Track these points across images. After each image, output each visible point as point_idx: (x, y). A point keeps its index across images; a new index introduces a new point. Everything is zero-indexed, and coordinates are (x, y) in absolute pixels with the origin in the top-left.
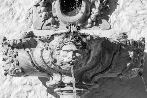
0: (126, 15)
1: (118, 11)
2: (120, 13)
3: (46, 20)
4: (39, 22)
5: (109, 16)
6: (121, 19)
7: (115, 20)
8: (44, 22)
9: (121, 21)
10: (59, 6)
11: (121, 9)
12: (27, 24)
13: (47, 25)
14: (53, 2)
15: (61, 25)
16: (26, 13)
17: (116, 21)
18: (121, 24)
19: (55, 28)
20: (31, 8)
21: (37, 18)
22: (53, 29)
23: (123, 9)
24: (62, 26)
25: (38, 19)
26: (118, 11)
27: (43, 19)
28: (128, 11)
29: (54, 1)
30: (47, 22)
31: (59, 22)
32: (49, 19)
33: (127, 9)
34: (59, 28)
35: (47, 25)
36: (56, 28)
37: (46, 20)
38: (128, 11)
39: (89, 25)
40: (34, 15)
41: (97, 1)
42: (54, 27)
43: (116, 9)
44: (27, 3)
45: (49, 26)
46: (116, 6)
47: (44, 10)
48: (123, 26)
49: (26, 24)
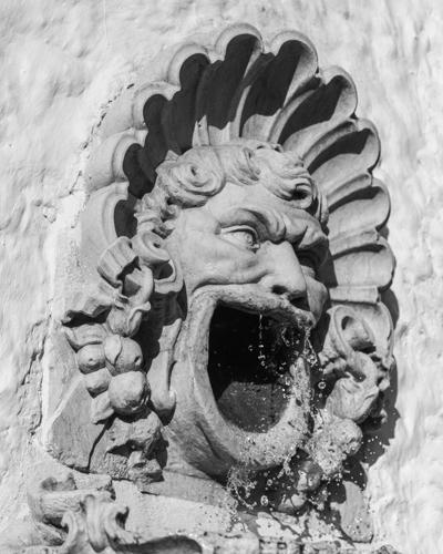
0: (432, 483)
1: (401, 453)
2: (404, 461)
3: (117, 422)
4: (82, 420)
5: (365, 466)
6: (412, 497)
7: (388, 498)
8: (102, 426)
9: (412, 510)
10: (205, 357)
11: (411, 447)
12: (21, 418)
13: (115, 451)
14: (169, 322)
15: (174, 466)
16: (17, 346)
17: (392, 502)
18: (408, 524)
19: (149, 475)
20: (37, 325)
21: (68, 395)
22: (135, 482)
23: (415, 447)
24: (175, 472)
25: (77, 399)
26: (401, 453)
27: (107, 408)
28: (436, 464)
29: (178, 321)
30: (122, 432)
31: (167, 444)
32: (146, 417)
33: (429, 448)
34: (161, 479)
35: (115, 451)
36: (157, 478)
37: (117, 422)
38: (434, 460)
39: (297, 500)
40: (51, 368)
41: (359, 377)
42: (146, 469)
43: (393, 437)
44: (17, 287)
45: (124, 460)
46: (394, 424)
47: (139, 362)
48: (415, 535)
49: (11, 418)
